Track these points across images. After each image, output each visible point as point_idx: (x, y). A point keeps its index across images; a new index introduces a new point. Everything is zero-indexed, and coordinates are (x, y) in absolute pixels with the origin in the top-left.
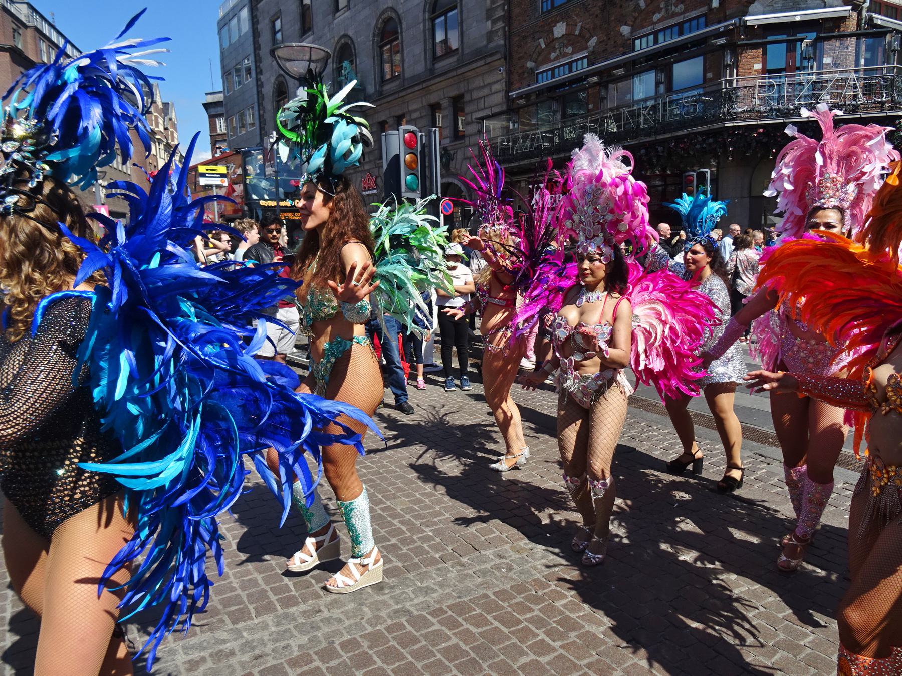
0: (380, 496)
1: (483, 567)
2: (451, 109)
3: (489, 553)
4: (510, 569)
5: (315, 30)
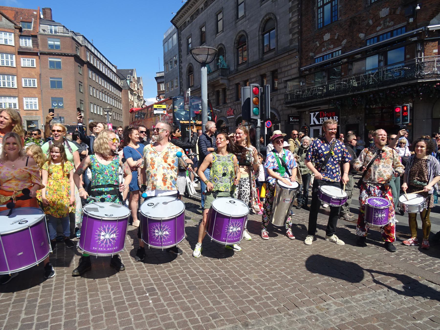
0: (242, 272)
1: (301, 317)
2: (271, 77)
3: (304, 309)
4: (317, 320)
5: (207, 42)
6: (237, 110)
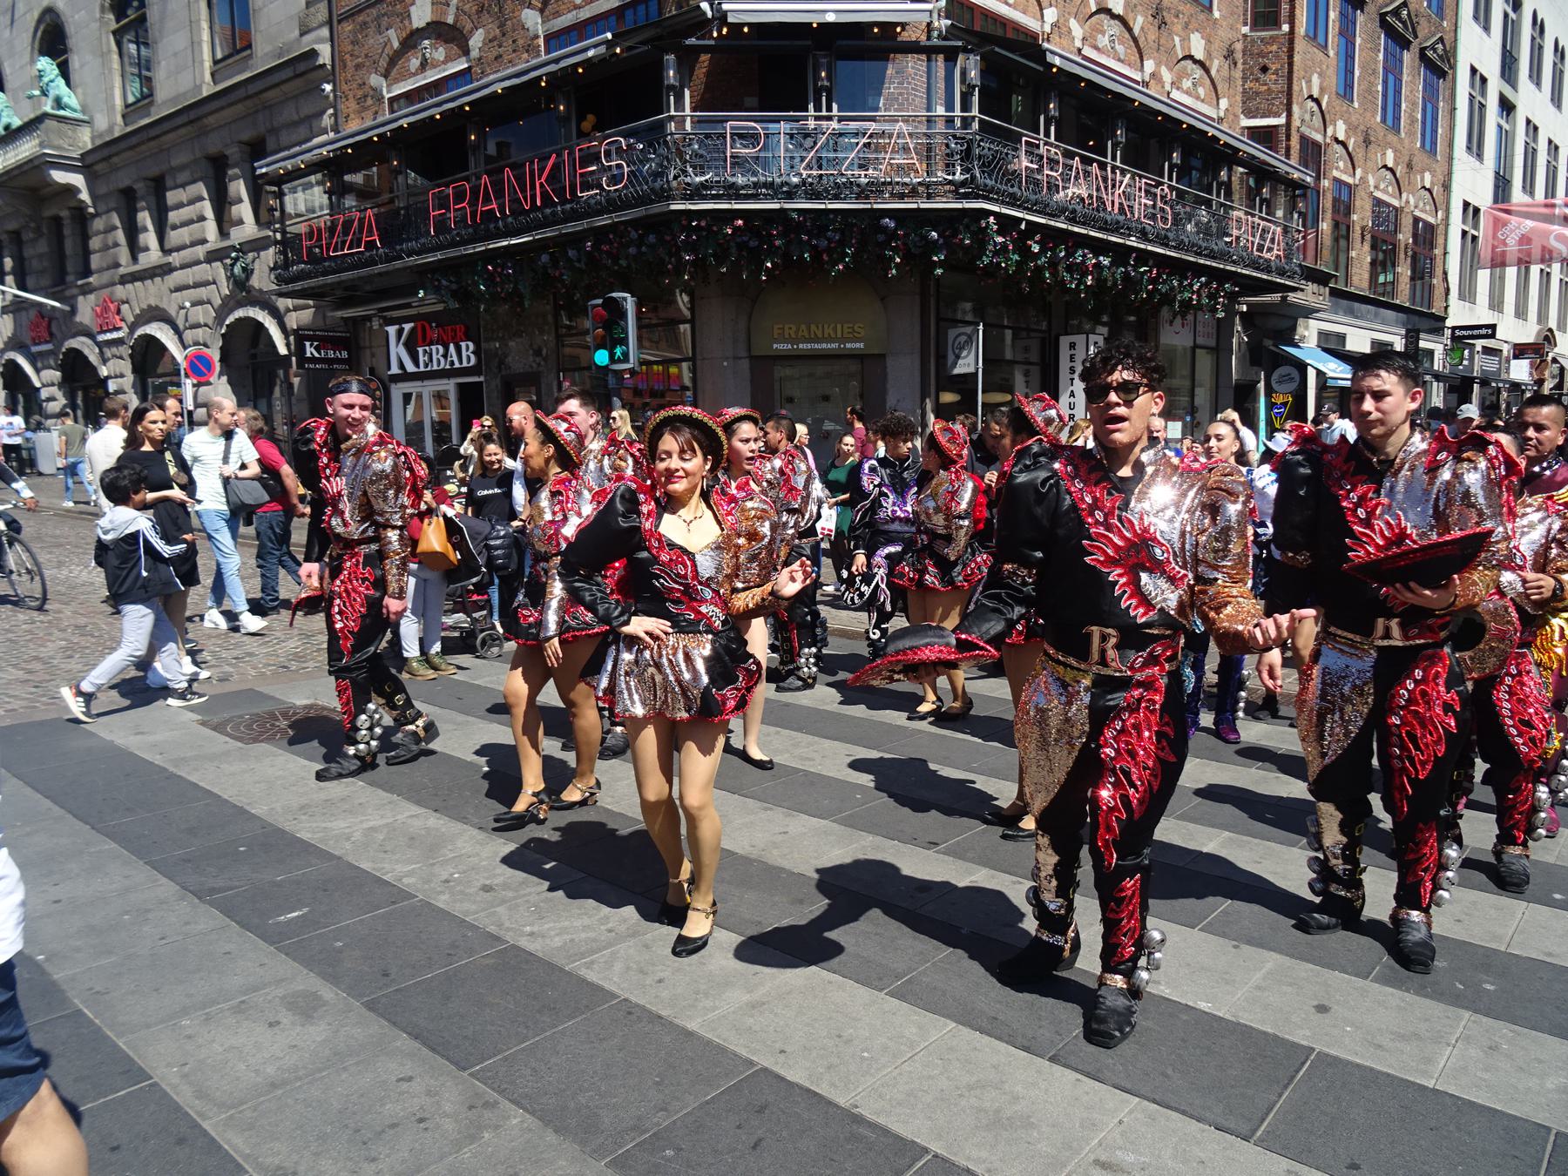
6: (134, 303)
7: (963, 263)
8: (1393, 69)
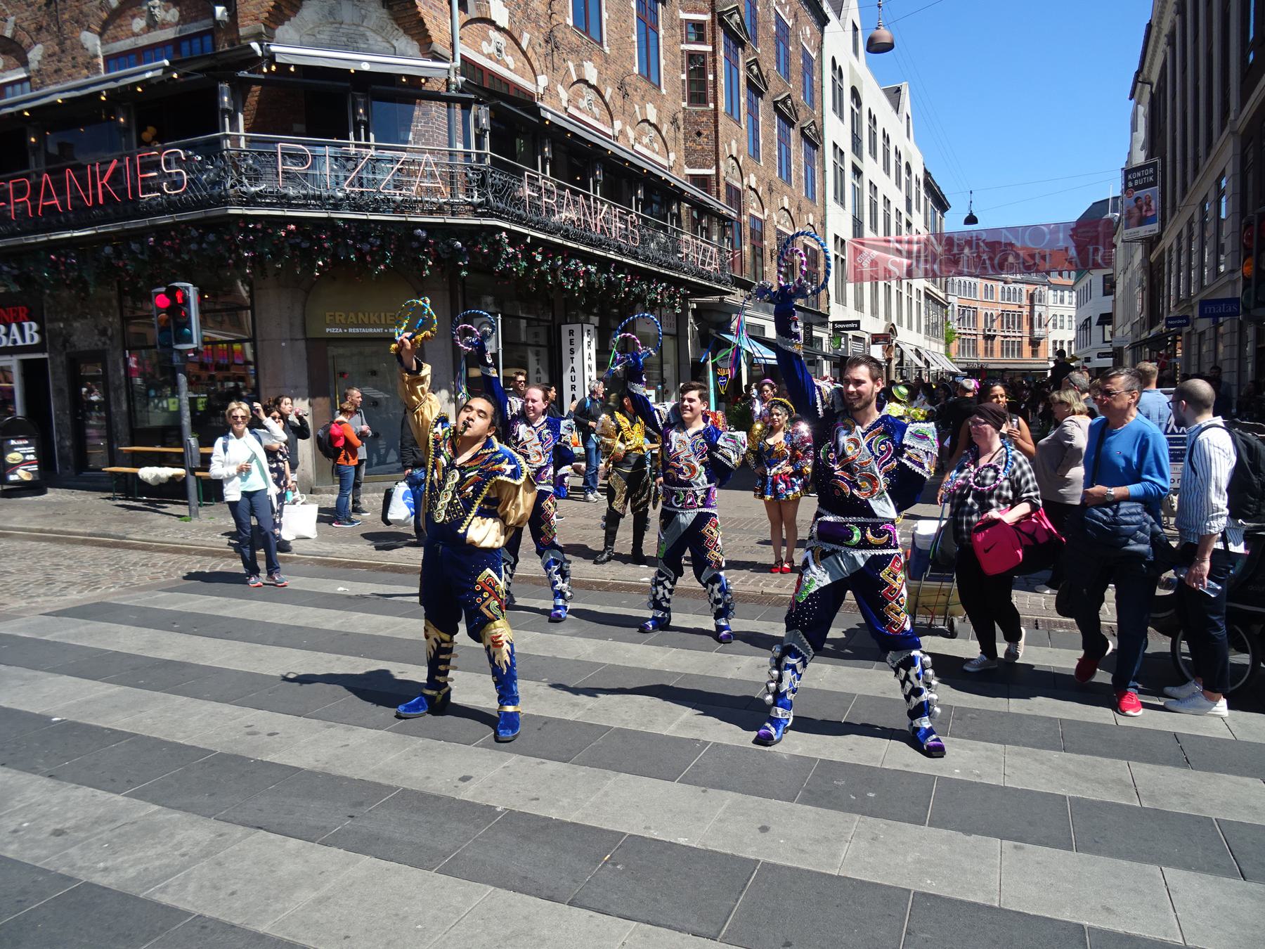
7: (483, 267)
8: (784, 140)
